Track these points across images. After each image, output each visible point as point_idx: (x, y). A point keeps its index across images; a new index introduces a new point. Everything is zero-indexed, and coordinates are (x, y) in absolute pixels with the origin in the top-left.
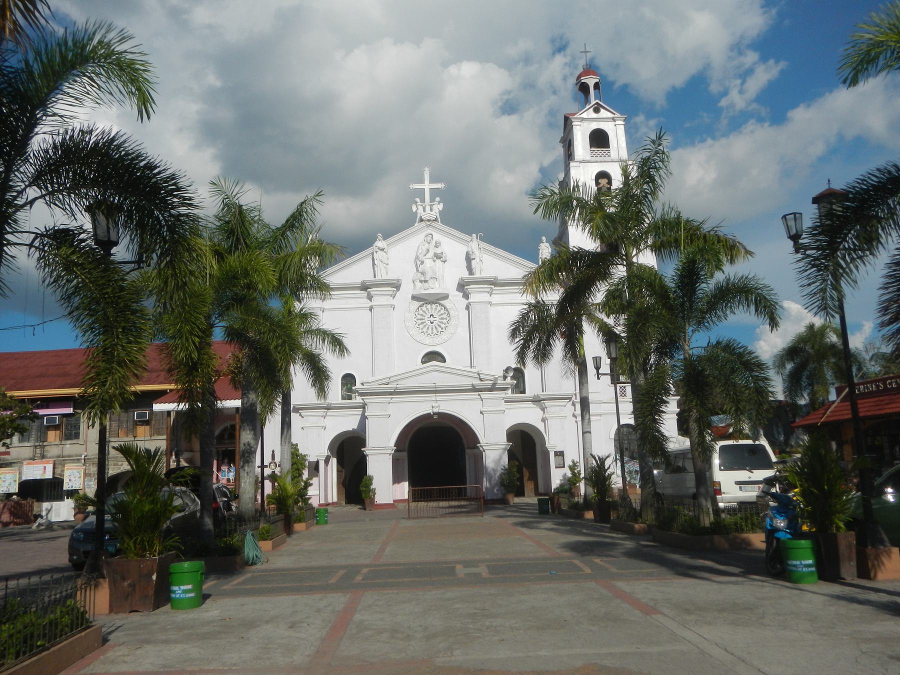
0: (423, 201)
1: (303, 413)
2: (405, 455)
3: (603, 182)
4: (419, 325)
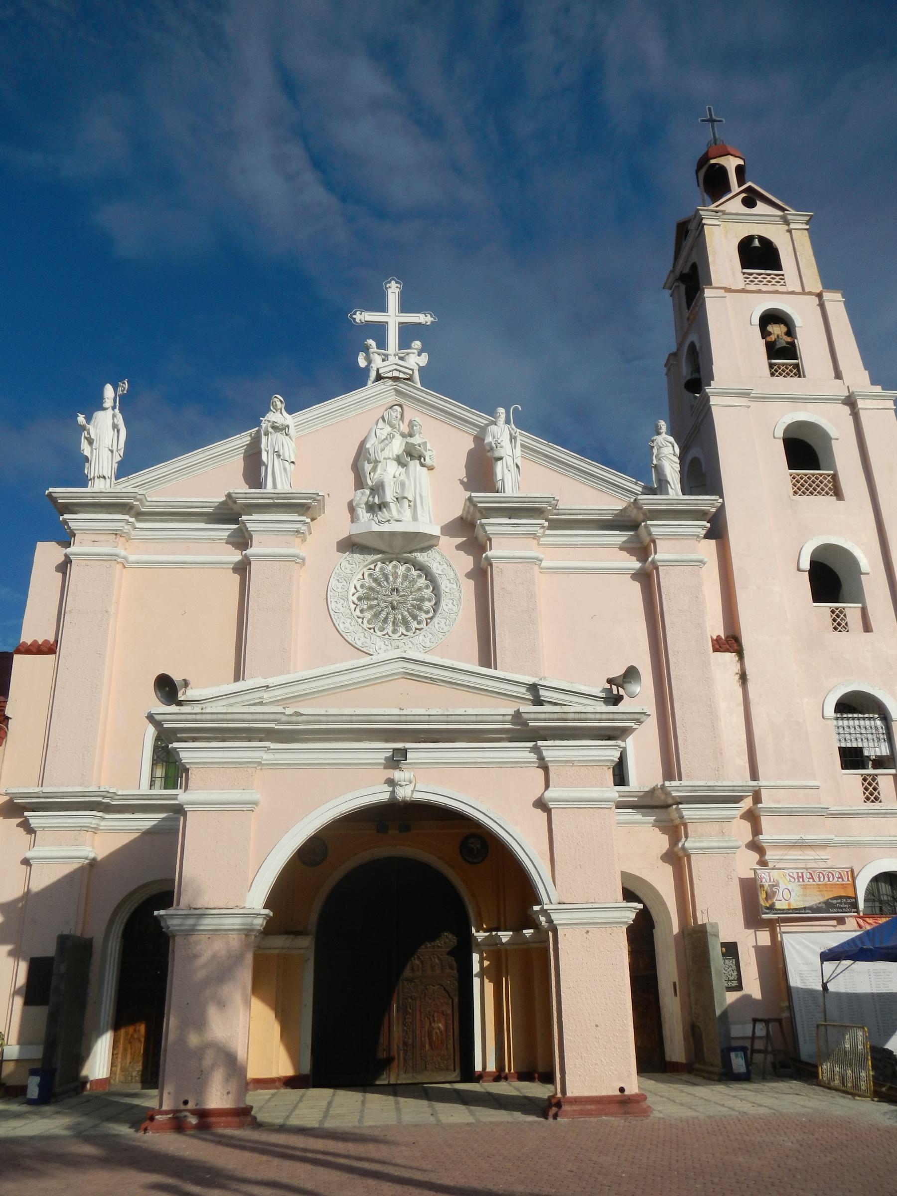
0: (382, 344)
1: (36, 819)
2: (305, 945)
3: (777, 330)
4: (362, 611)
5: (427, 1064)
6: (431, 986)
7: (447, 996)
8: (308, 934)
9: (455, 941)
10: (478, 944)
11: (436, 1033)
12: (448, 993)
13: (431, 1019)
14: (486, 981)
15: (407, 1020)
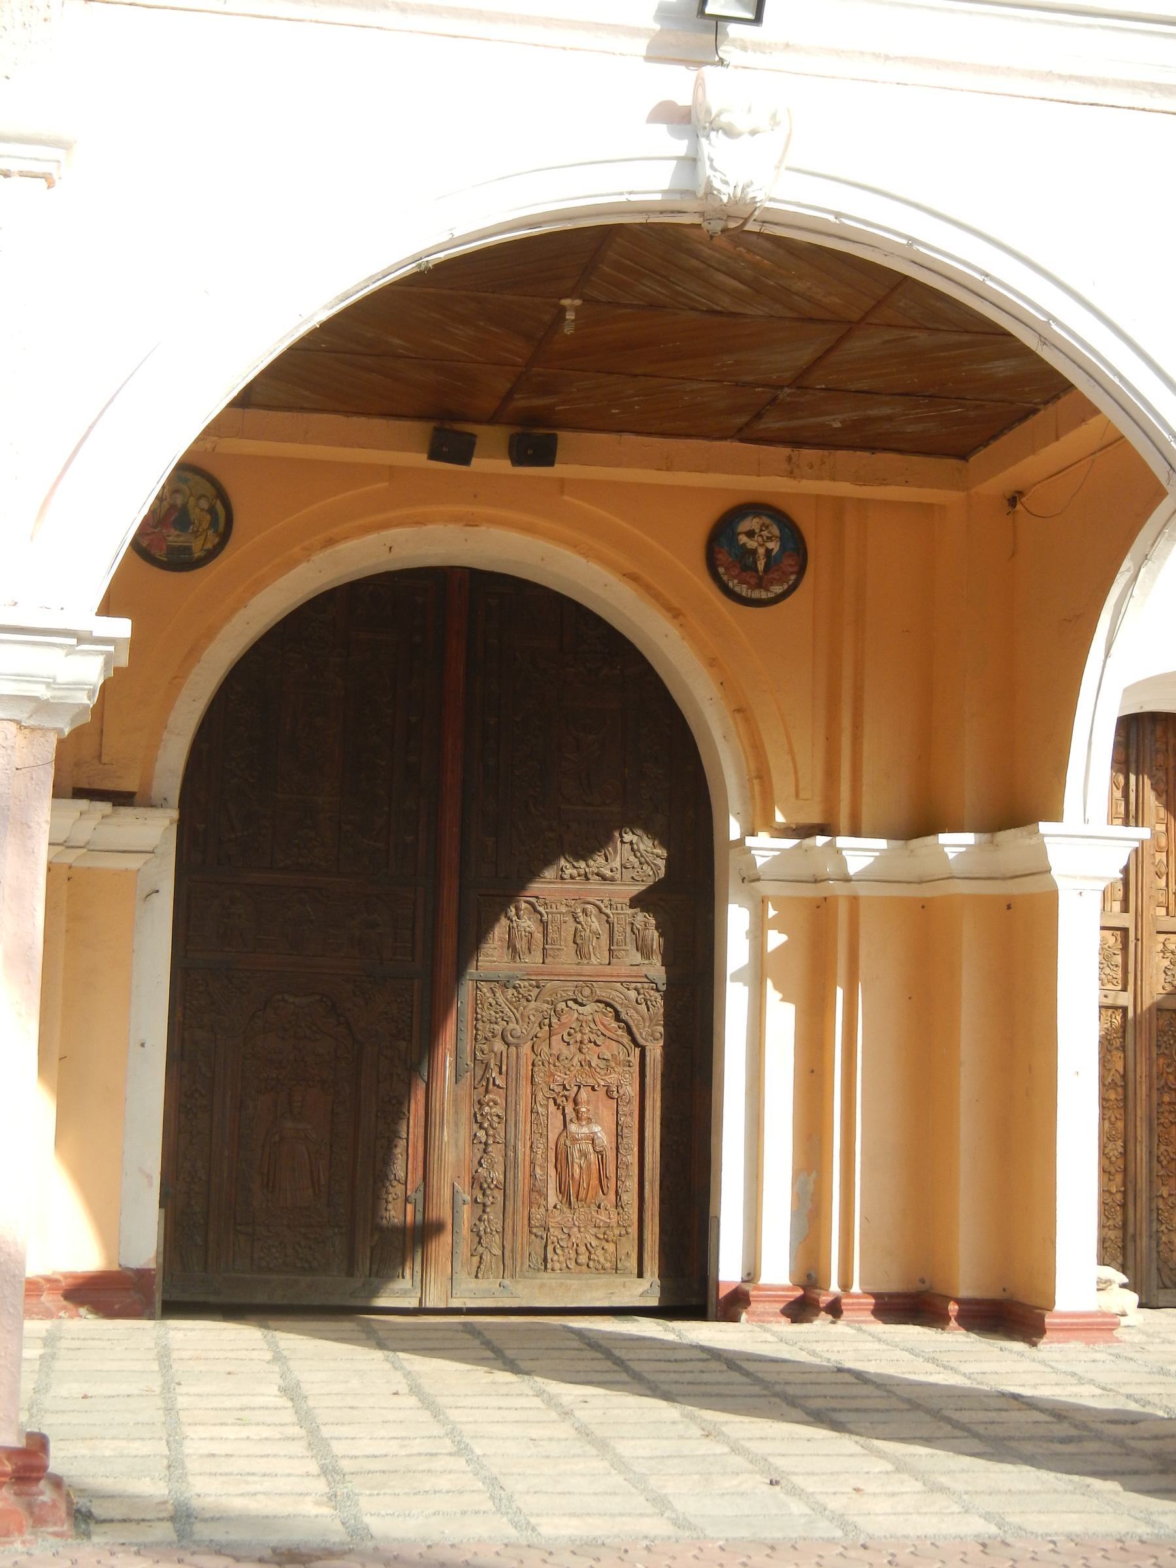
5: (550, 1248)
6: (570, 1003)
7: (626, 1040)
8: (149, 804)
9: (661, 863)
10: (751, 878)
11: (584, 1155)
12: (630, 1031)
13: (569, 1109)
14: (772, 995)
15: (487, 1109)
